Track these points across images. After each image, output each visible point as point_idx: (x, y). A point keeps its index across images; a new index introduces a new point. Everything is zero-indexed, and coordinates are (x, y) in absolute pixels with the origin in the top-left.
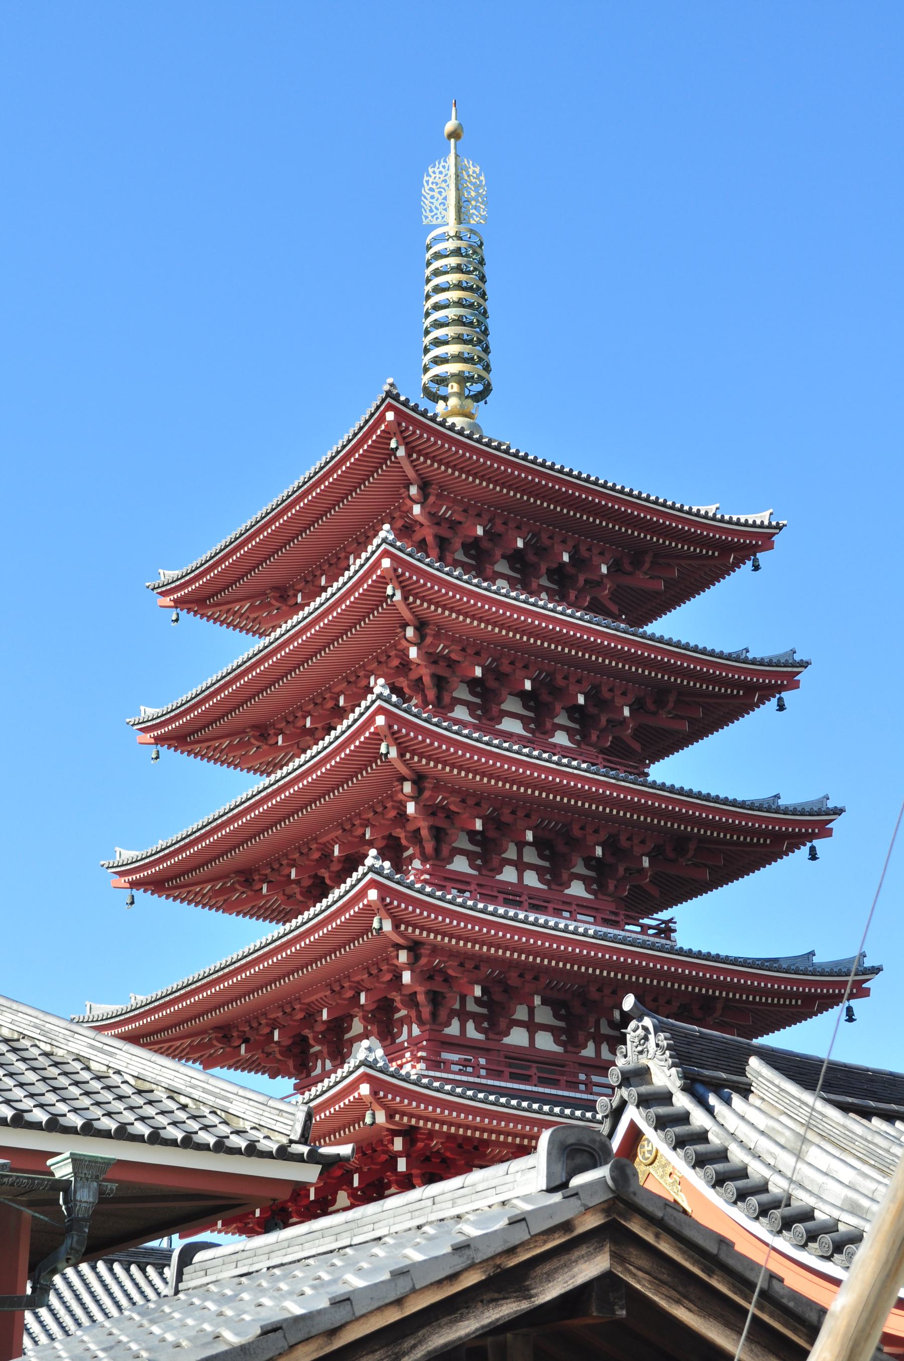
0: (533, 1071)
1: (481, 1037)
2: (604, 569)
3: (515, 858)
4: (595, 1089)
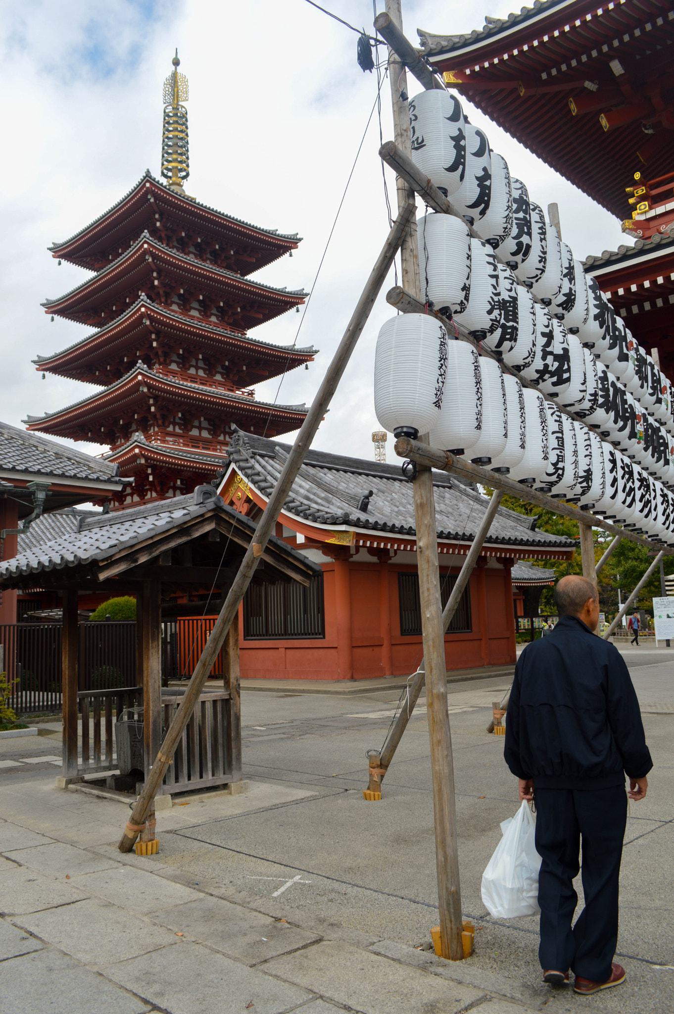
2: (232, 253)
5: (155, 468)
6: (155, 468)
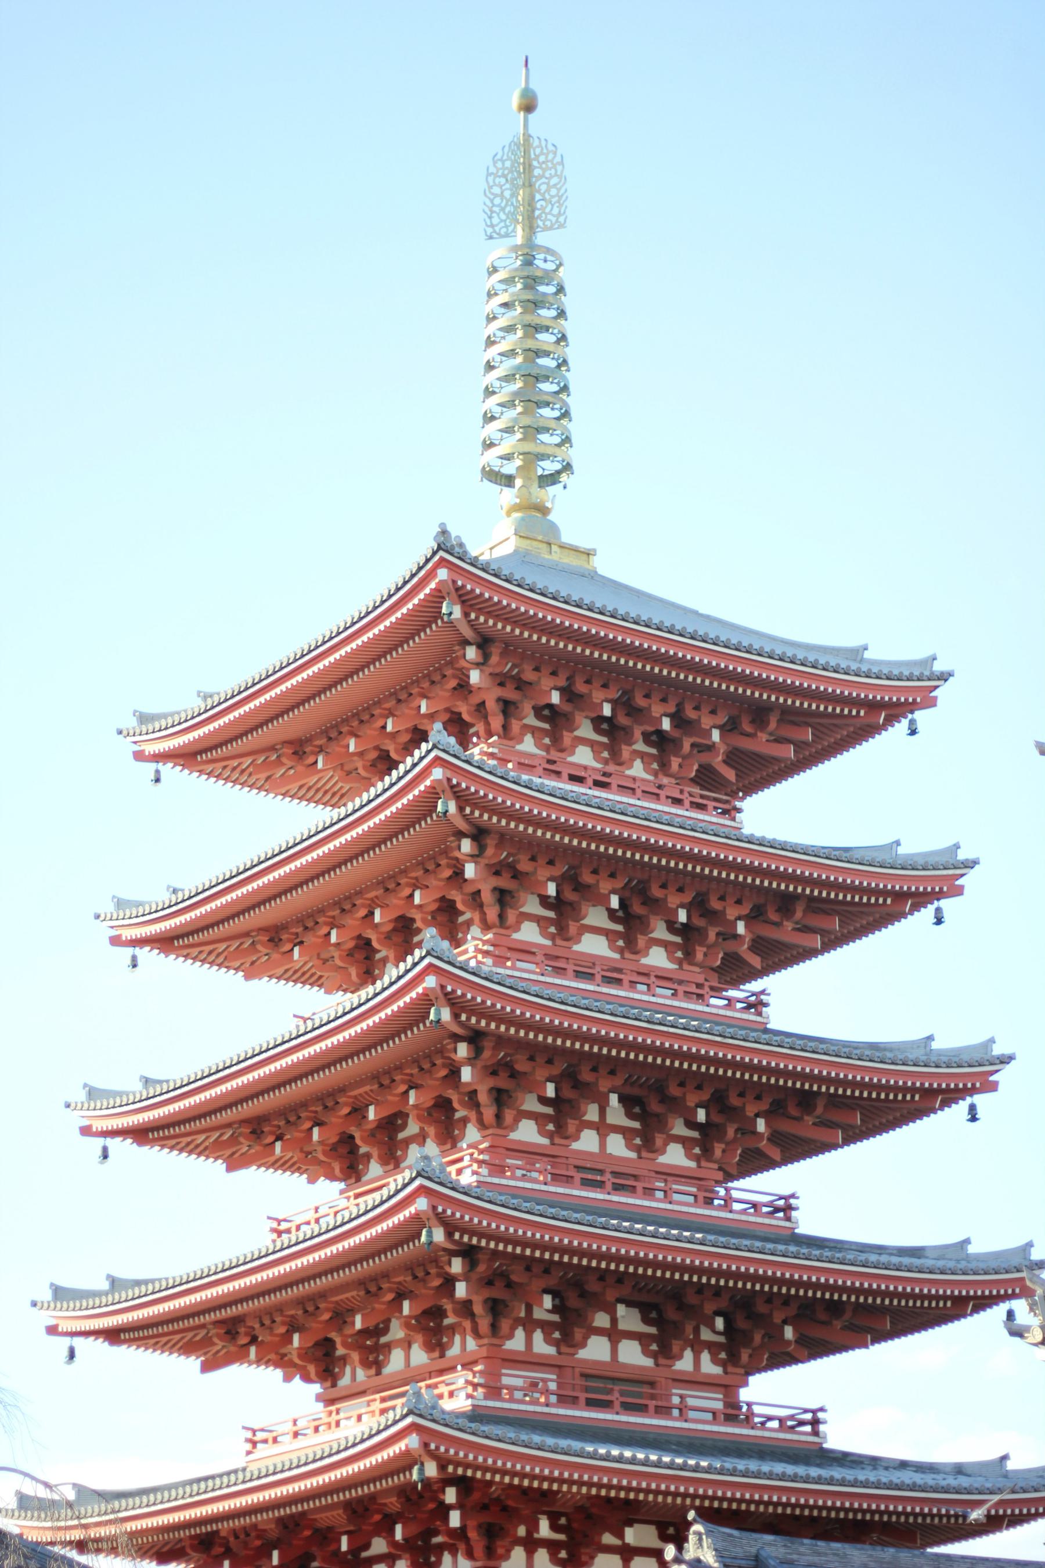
0: (615, 1396)
4: (692, 1414)
5: (464, 1485)
6: (464, 1485)
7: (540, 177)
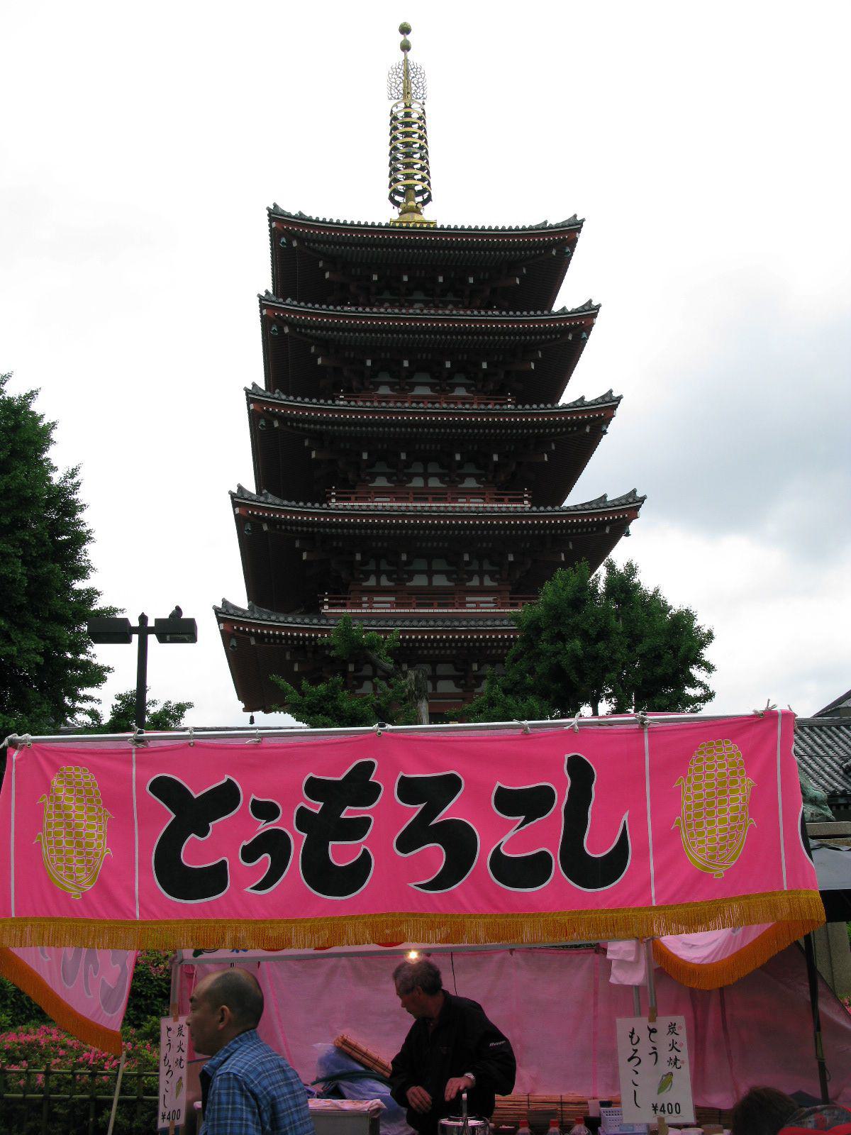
1: (392, 584)
3: (421, 471)
4: (468, 605)
7: (413, 77)
